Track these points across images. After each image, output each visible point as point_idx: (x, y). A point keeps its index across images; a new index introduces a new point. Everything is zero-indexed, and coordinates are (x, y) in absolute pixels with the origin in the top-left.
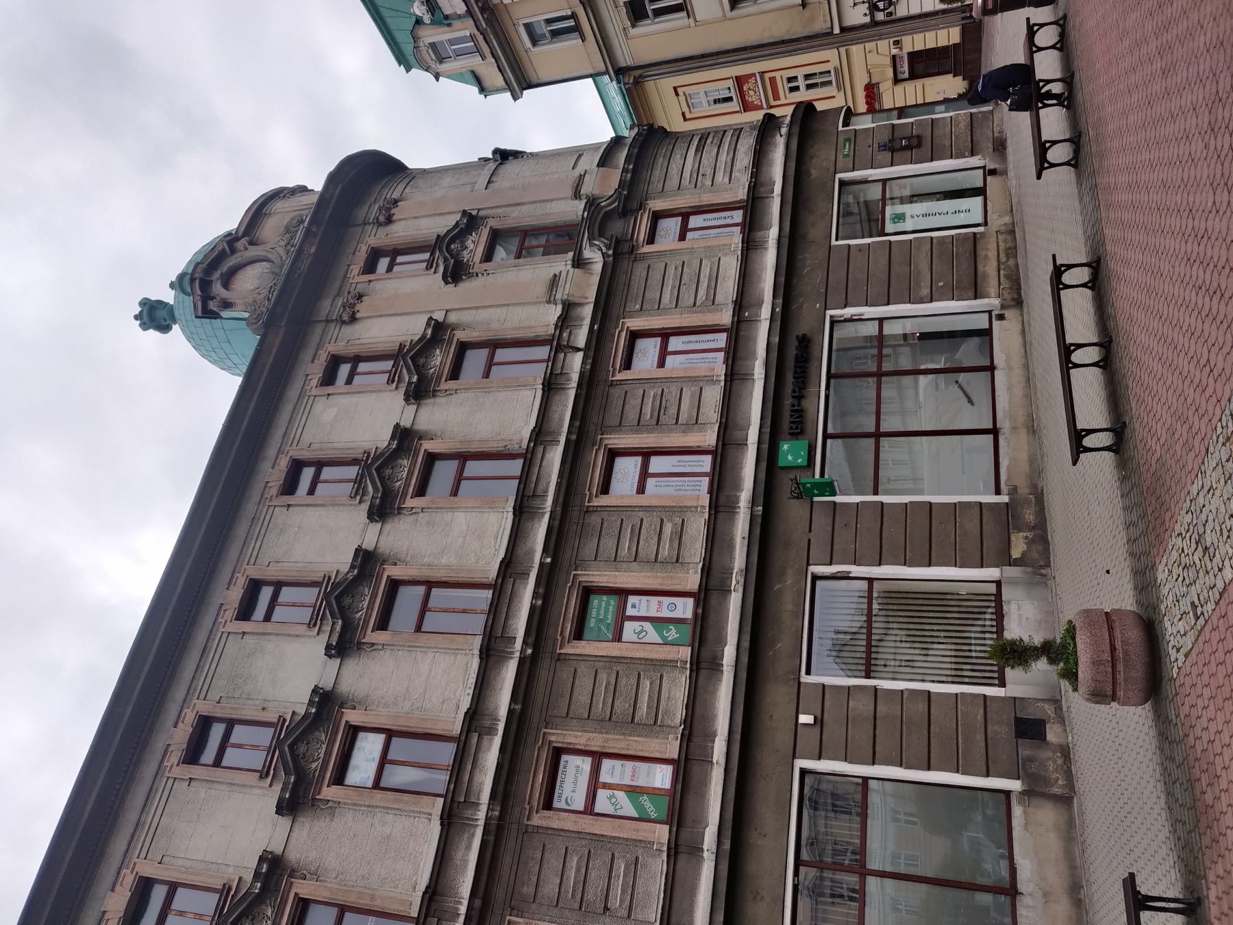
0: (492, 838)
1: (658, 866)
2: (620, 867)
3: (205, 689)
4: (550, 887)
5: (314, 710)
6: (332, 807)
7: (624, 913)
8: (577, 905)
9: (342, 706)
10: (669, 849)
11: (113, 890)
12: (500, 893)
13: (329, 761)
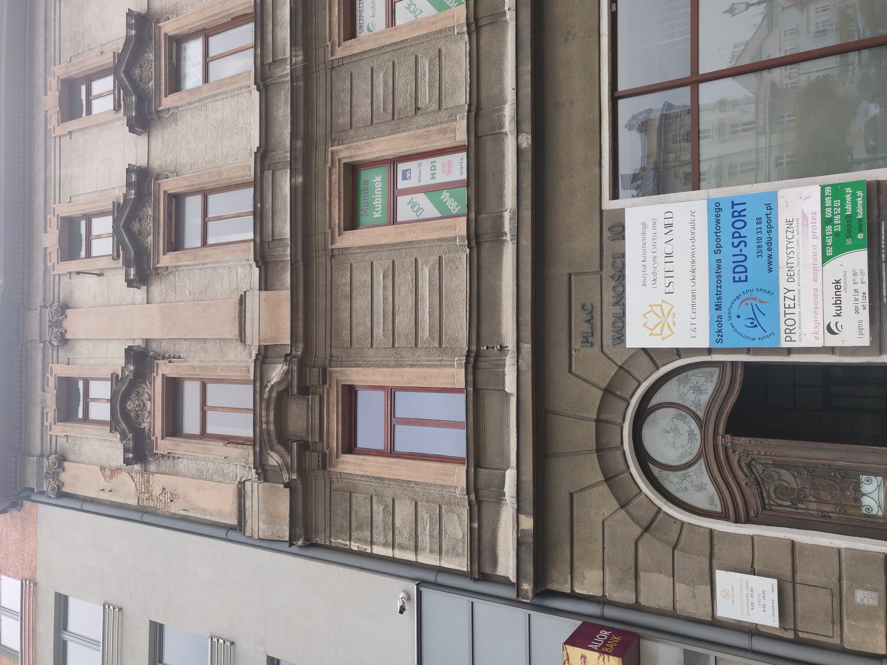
0: (301, 83)
1: (461, 49)
2: (424, 64)
3: (57, 57)
4: (363, 110)
5: (133, 32)
6: (173, 114)
7: (435, 106)
8: (390, 117)
9: (158, 21)
10: (468, 25)
11: (46, 232)
12: (320, 131)
13: (160, 75)
